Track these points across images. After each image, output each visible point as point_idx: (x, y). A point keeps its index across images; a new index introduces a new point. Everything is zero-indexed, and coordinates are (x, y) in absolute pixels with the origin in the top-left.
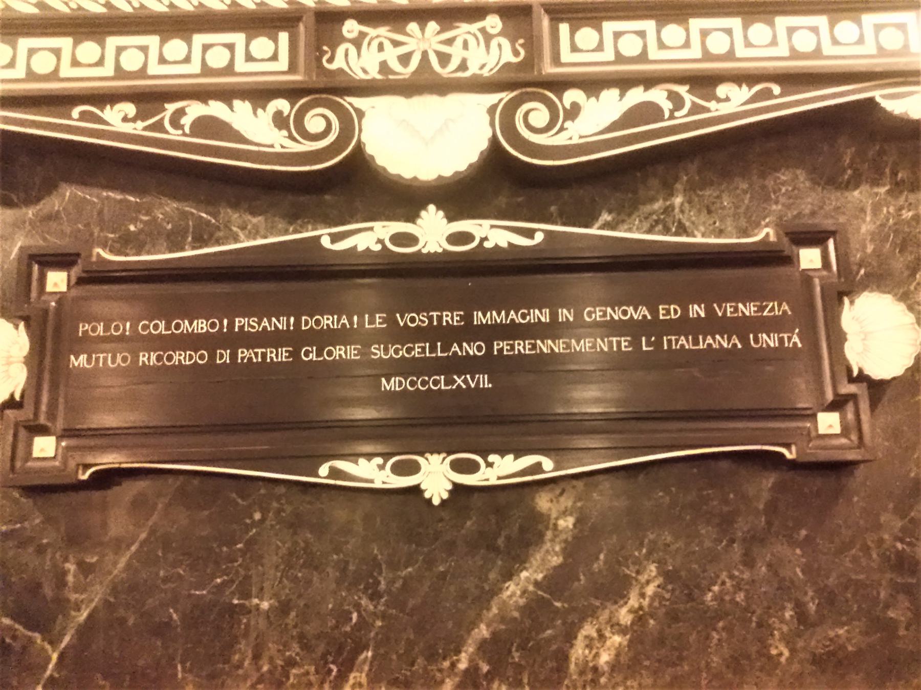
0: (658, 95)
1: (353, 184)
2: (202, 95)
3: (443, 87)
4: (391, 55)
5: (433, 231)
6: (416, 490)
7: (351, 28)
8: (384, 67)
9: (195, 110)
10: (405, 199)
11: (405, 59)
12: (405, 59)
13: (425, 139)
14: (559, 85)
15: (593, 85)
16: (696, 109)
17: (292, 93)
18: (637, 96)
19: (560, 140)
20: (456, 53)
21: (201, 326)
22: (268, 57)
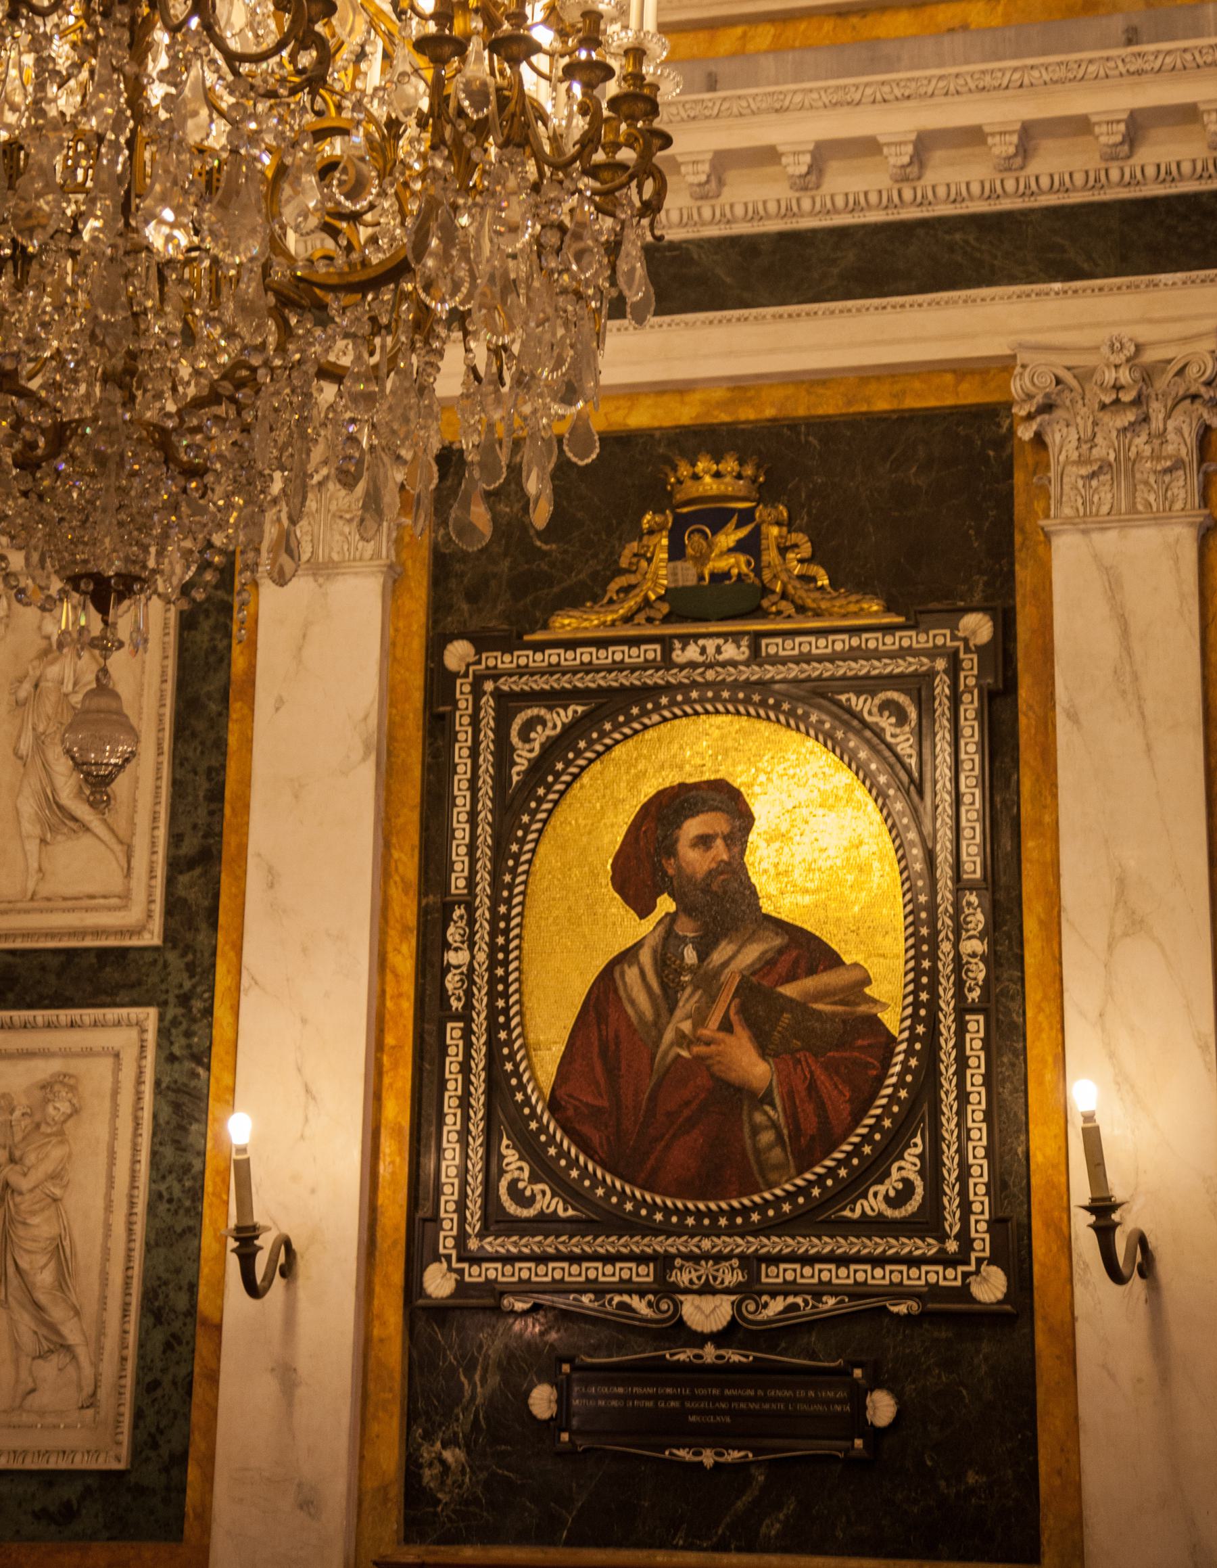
0: (799, 1300)
1: (679, 1332)
2: (620, 1292)
3: (714, 1292)
4: (694, 1275)
5: (709, 1353)
6: (701, 1463)
7: (678, 1262)
8: (691, 1282)
9: (617, 1299)
10: (700, 1339)
11: (699, 1278)
12: (699, 1278)
13: (707, 1313)
14: (760, 1294)
15: (773, 1295)
16: (814, 1307)
17: (655, 1293)
18: (791, 1299)
19: (759, 1318)
20: (720, 1274)
21: (621, 1390)
22: (644, 1274)
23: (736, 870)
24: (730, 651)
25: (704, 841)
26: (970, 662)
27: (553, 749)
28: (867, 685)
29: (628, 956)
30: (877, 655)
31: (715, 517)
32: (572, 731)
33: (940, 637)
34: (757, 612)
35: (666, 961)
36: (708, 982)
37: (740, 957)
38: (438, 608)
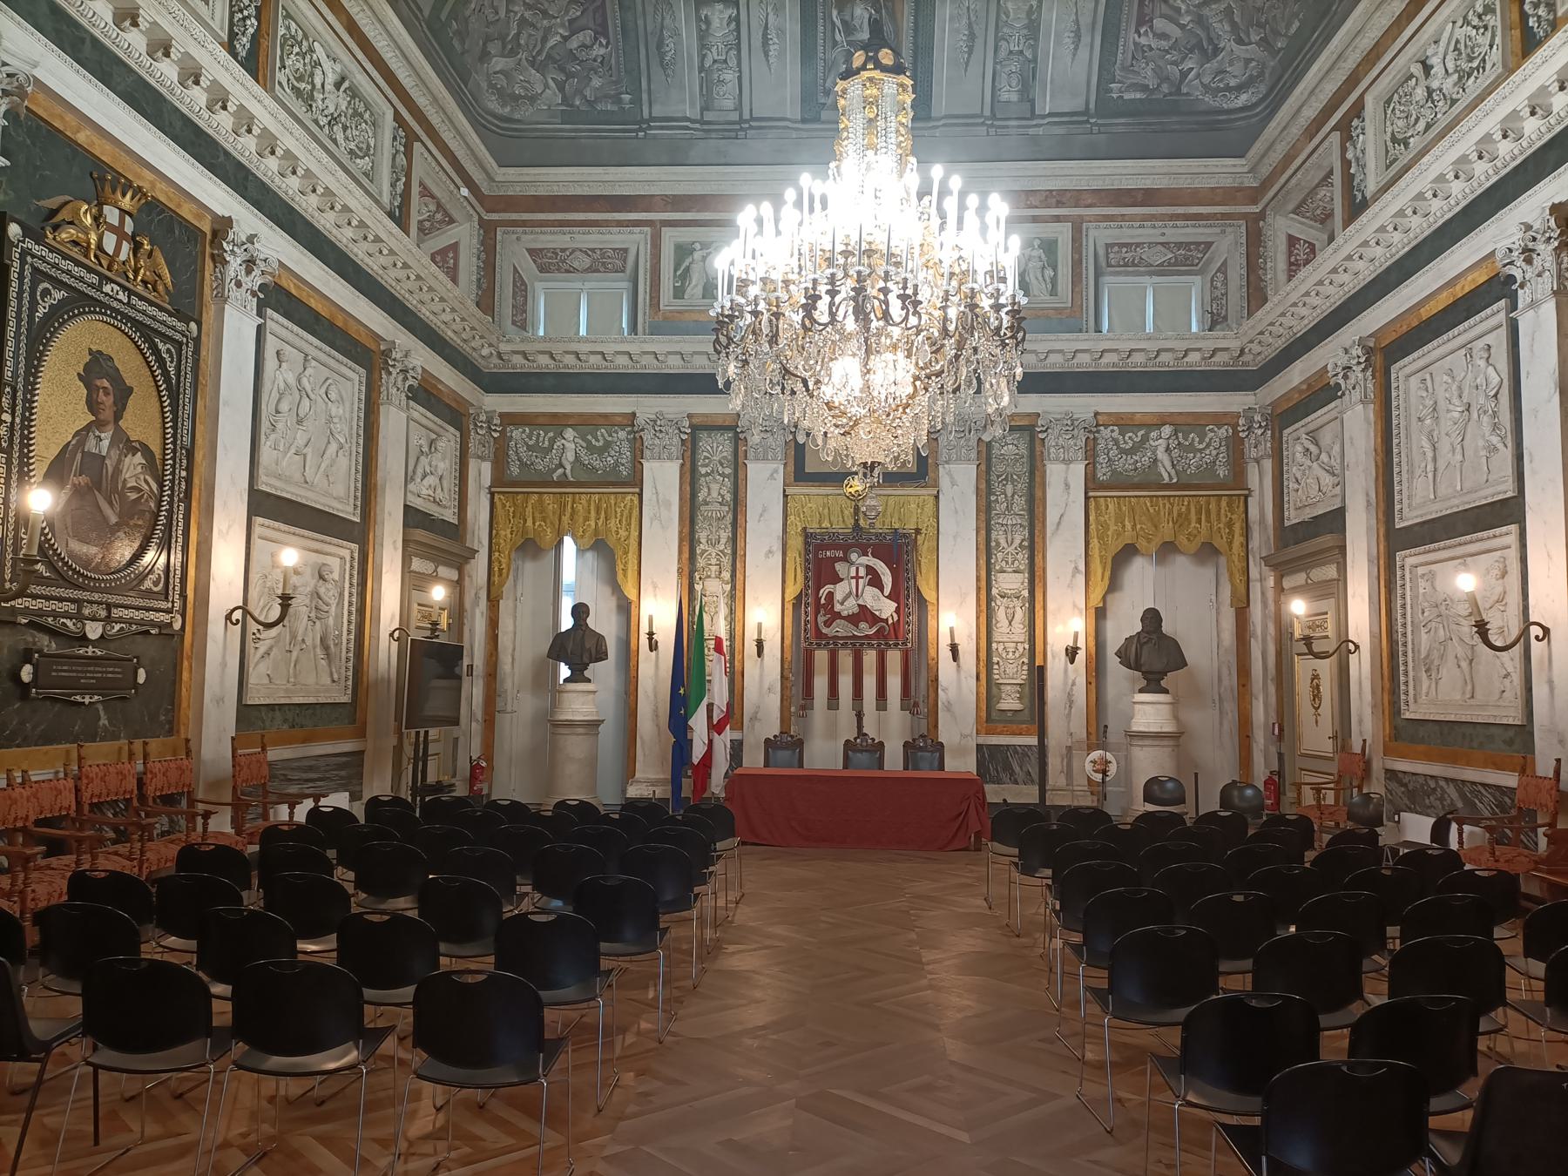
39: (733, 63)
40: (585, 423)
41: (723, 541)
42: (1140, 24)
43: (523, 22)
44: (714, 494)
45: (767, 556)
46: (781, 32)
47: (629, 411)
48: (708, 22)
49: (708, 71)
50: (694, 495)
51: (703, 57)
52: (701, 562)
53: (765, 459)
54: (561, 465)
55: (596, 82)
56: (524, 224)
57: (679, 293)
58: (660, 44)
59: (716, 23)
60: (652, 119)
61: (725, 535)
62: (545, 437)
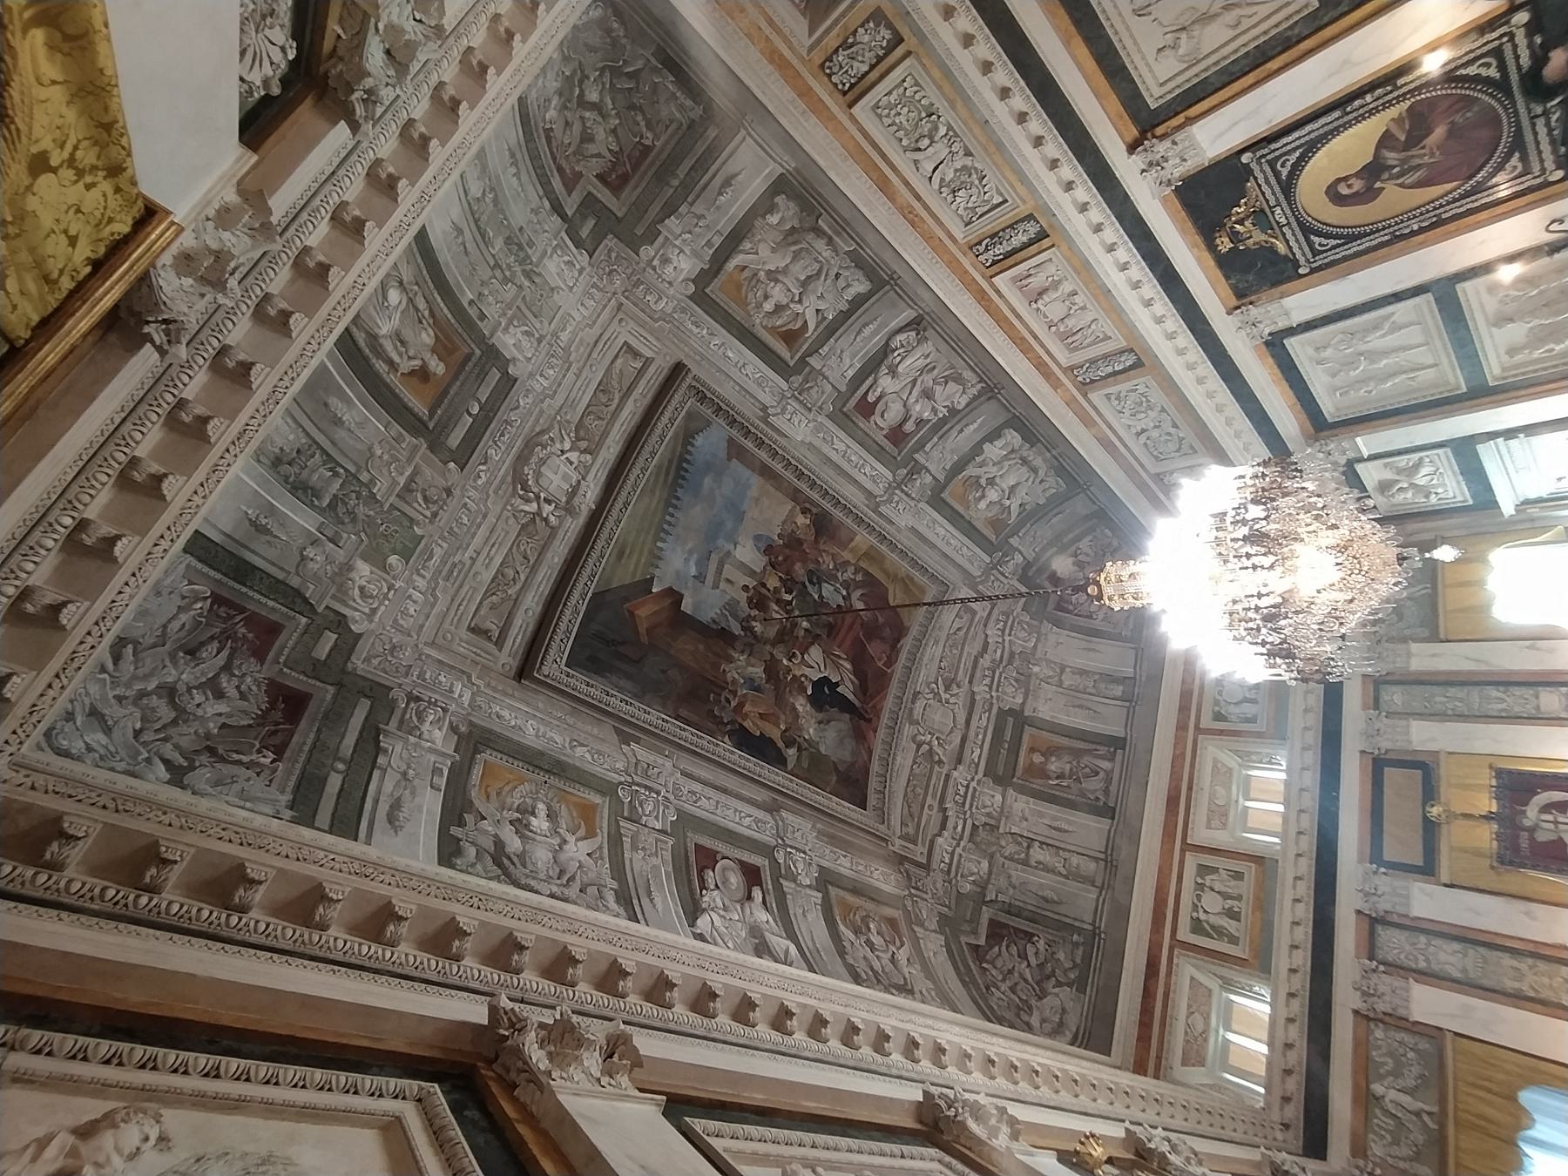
23: (1357, 175)
24: (1278, 210)
25: (1349, 186)
26: (1259, 154)
27: (1328, 236)
28: (1277, 174)
29: (1400, 185)
30: (1266, 179)
31: (1235, 237)
32: (1319, 234)
33: (1254, 166)
34: (1262, 211)
35: (1399, 176)
36: (1403, 161)
37: (1391, 157)
38: (1289, 279)
39: (1067, 855)
40: (1364, 1069)
41: (1515, 963)
42: (1090, 617)
43: (1013, 989)
44: (1452, 959)
45: (1534, 919)
46: (1055, 819)
47: (1351, 1016)
48: (1039, 863)
49: (1069, 872)
50: (1455, 981)
51: (1060, 874)
52: (1545, 994)
53: (1408, 897)
54: (1418, 1114)
55: (1061, 956)
56: (1159, 1058)
57: (1234, 940)
58: (1046, 900)
59: (1041, 858)
60: (1093, 924)
61: (1507, 961)
62: (1380, 1119)
